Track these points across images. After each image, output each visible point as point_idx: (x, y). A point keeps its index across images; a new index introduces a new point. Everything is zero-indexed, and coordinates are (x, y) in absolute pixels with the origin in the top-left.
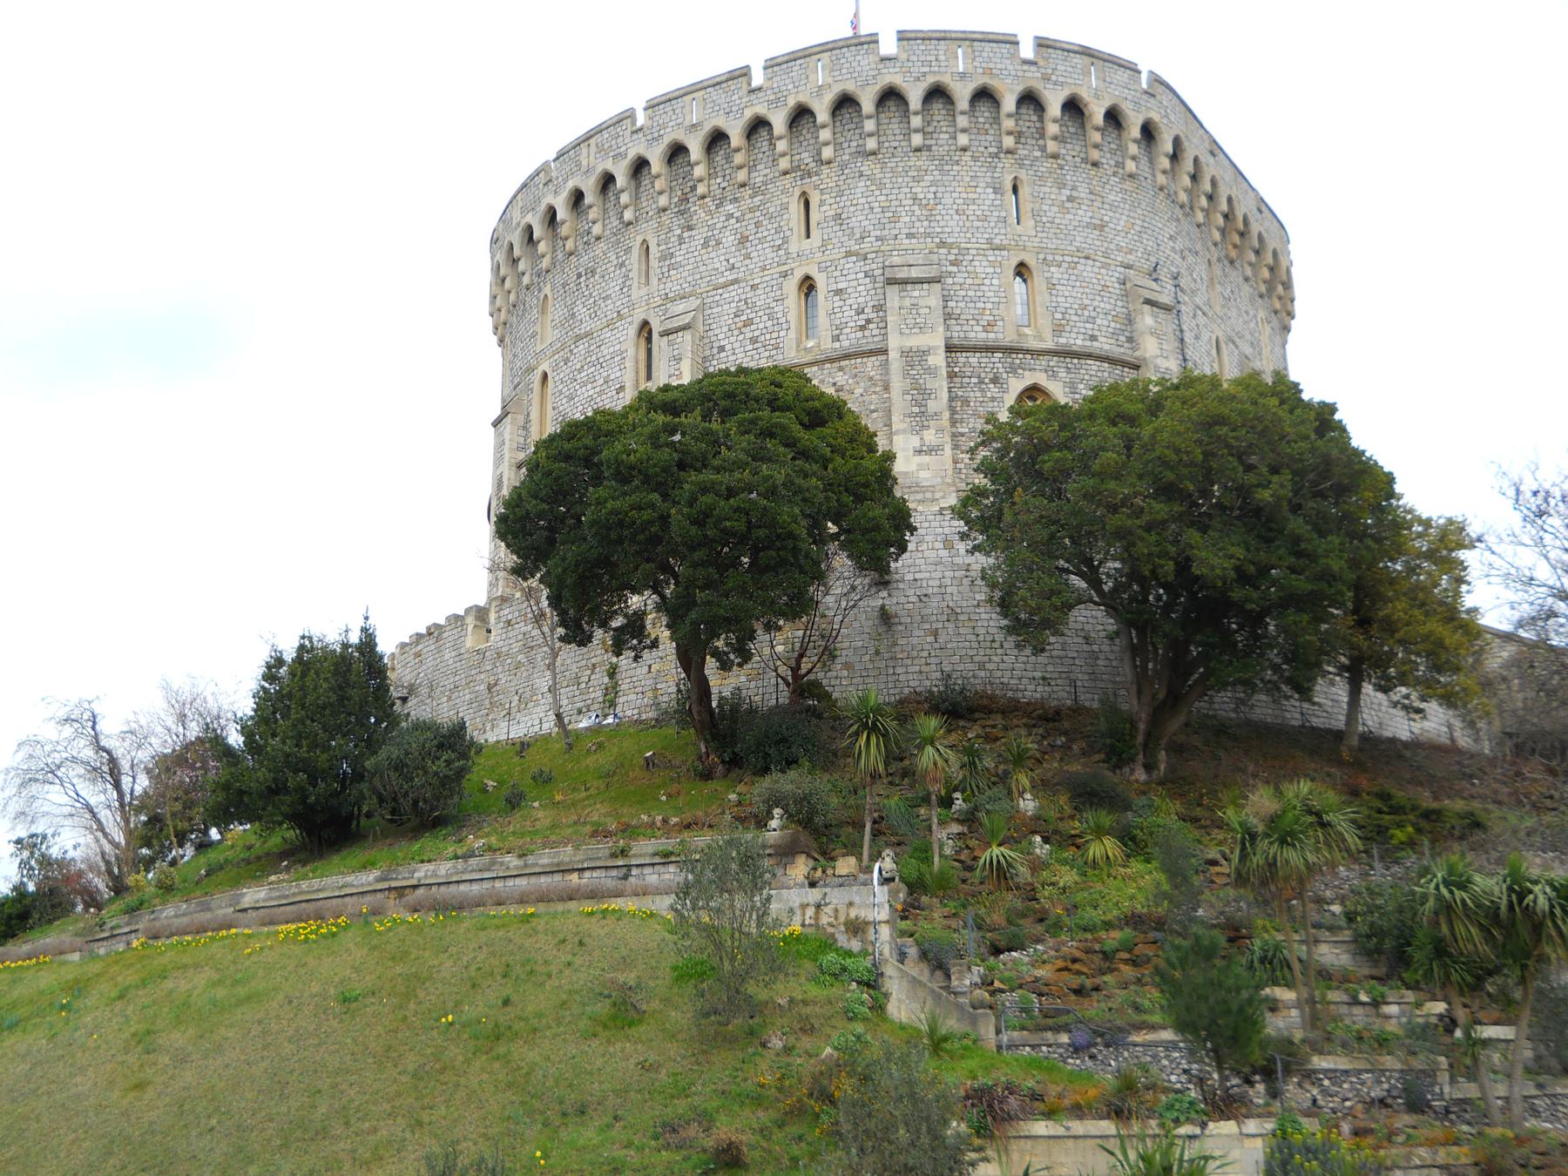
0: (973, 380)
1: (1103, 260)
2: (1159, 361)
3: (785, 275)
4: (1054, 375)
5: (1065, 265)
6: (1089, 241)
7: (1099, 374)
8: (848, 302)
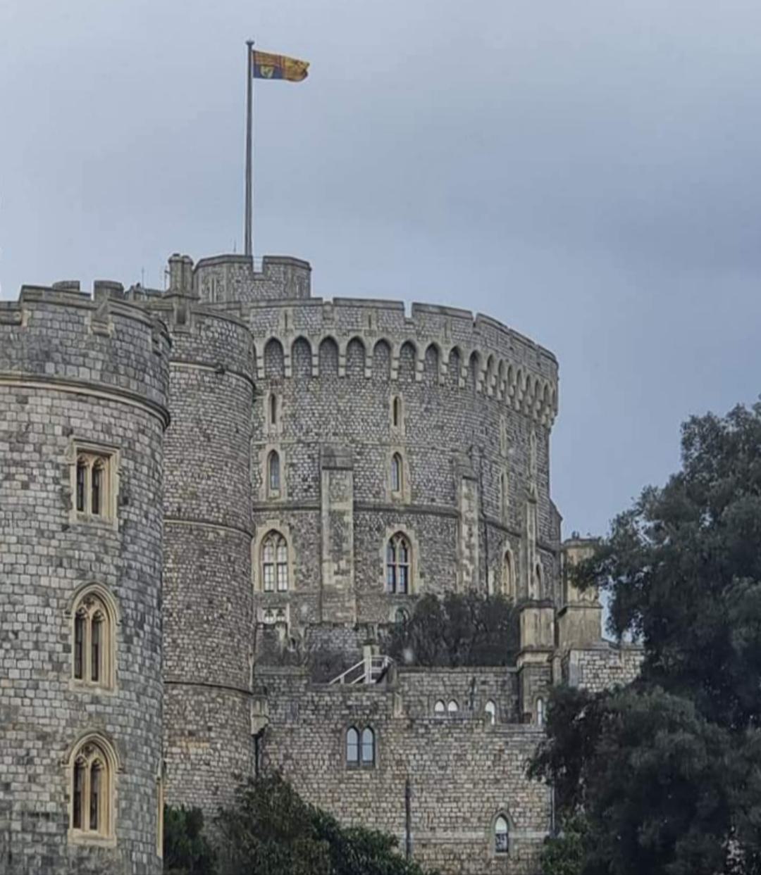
2: (467, 515)
3: (260, 447)
4: (410, 526)
8: (299, 472)
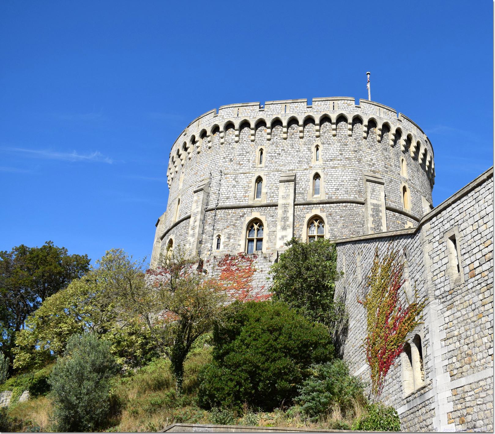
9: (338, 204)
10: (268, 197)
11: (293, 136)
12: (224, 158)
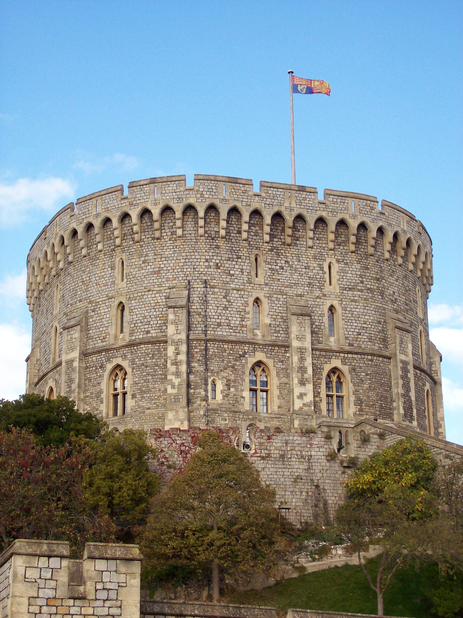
0: (94, 368)
1: (158, 289)
2: (174, 337)
4: (124, 357)
5: (138, 298)
6: (151, 281)
7: (146, 351)
9: (363, 356)
10: (272, 331)
11: (298, 242)
12: (207, 260)
